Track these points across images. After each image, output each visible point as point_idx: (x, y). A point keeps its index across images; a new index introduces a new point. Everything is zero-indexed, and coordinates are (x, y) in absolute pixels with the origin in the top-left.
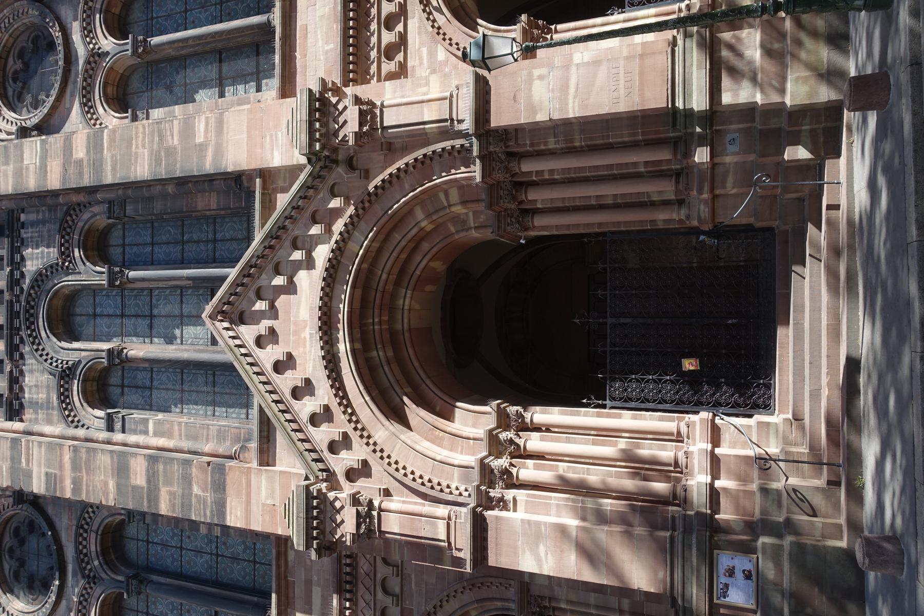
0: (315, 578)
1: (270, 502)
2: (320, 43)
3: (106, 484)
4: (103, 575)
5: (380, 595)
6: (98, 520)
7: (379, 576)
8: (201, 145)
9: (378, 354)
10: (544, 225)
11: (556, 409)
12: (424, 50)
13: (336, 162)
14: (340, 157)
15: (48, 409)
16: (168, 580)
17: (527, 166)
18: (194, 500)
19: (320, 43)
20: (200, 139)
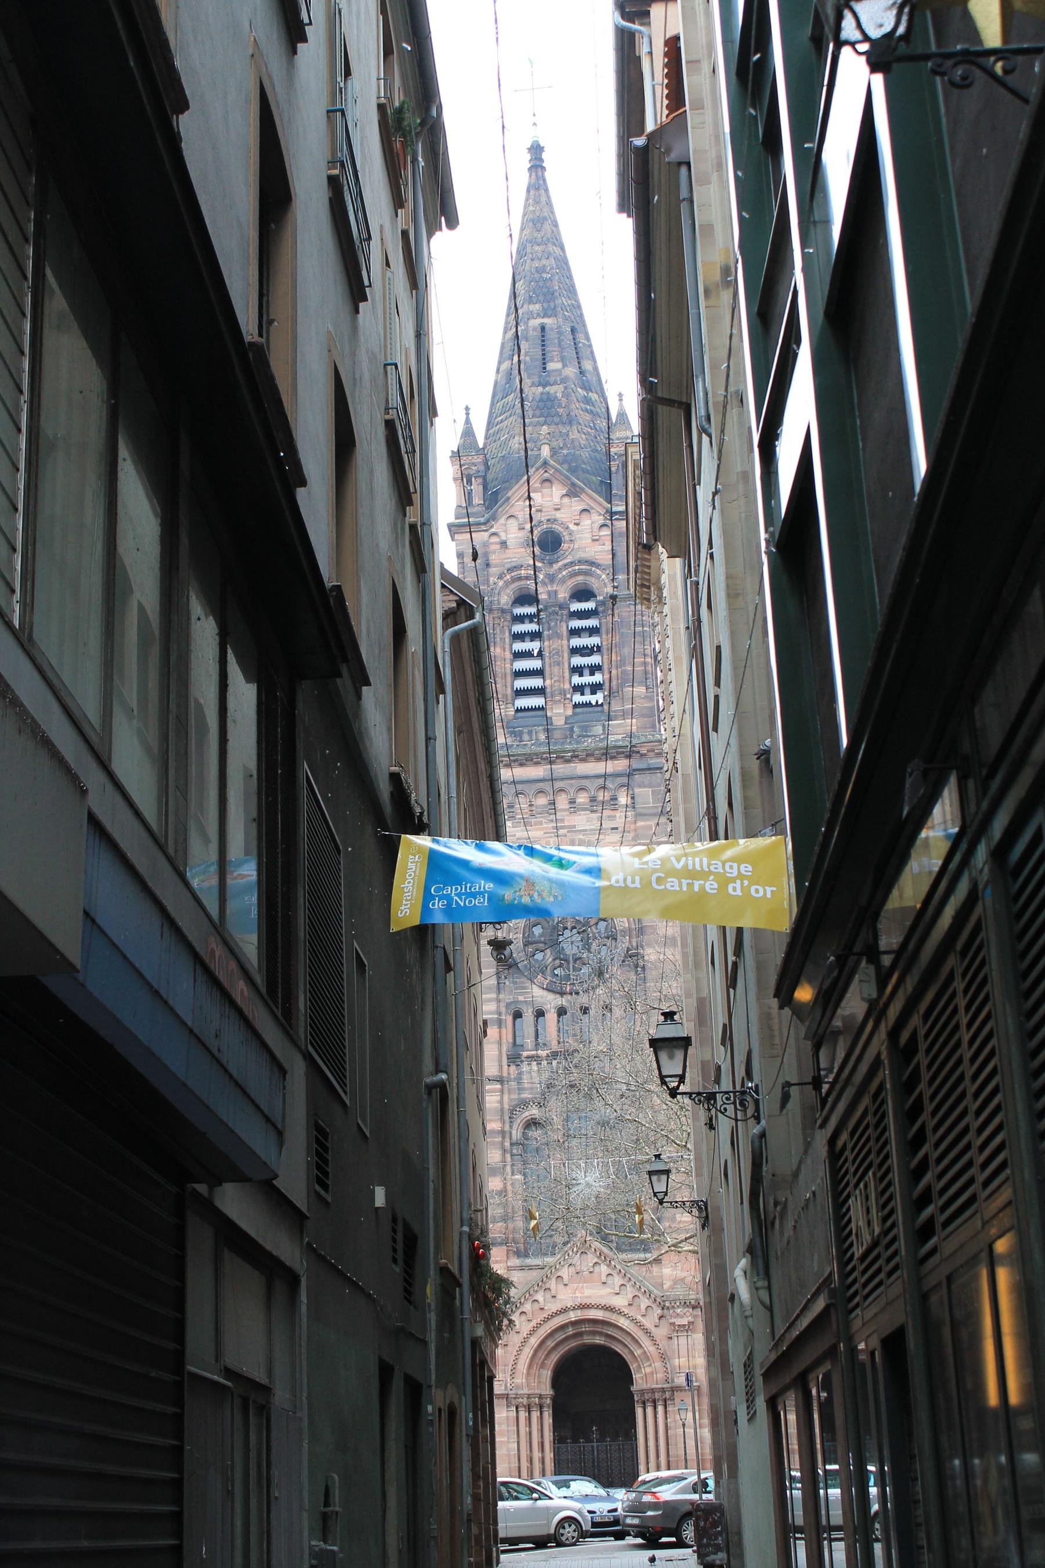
9: (570, 1331)
10: (639, 1411)
13: (663, 1309)
14: (665, 1311)
15: (519, 1089)
17: (660, 1409)
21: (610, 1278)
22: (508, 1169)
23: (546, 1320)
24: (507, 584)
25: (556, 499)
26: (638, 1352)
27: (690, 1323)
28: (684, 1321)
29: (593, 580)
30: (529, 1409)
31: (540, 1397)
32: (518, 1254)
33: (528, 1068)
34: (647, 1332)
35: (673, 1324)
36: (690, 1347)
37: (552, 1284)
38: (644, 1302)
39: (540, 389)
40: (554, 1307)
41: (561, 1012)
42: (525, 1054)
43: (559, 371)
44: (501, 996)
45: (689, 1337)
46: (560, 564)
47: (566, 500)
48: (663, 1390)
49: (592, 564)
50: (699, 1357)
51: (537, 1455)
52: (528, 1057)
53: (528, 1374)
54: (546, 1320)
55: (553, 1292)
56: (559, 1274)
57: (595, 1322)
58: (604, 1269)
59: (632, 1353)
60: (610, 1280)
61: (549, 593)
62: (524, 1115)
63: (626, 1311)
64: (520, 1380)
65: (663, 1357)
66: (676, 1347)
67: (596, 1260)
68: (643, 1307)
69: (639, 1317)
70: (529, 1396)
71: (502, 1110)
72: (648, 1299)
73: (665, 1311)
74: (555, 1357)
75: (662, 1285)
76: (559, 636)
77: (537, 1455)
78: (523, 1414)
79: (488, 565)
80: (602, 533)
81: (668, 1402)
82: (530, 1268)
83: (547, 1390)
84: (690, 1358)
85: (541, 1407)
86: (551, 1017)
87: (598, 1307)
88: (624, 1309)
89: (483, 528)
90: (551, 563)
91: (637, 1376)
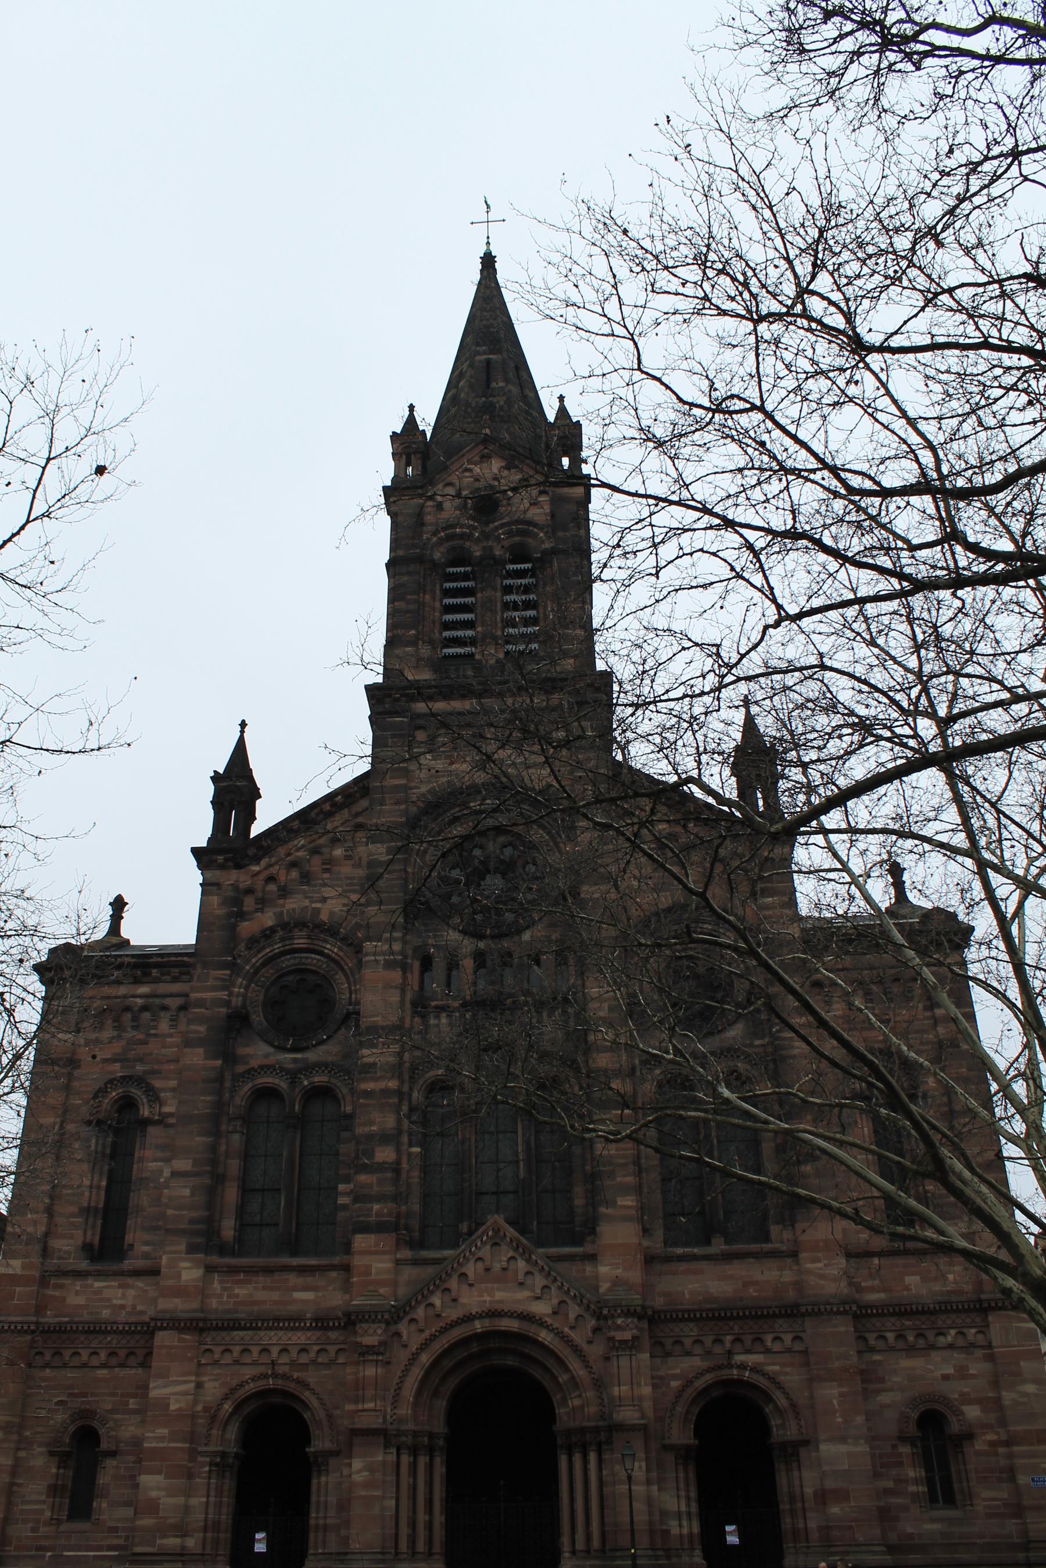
0: (320, 1294)
1: (373, 1270)
2: (690, 1286)
3: (372, 1123)
4: (297, 1090)
5: (316, 1348)
6: (339, 1084)
7: (328, 1347)
8: (615, 1202)
9: (475, 1348)
10: (563, 1460)
11: (444, 1470)
12: (678, 1371)
13: (598, 1319)
16: (298, 1149)
17: (592, 1456)
18: (369, 1205)
19: (690, 1286)
20: (621, 1201)
21: (529, 1277)
22: (405, 1139)
23: (443, 1330)
24: (441, 541)
25: (495, 470)
26: (563, 1378)
27: (635, 1338)
28: (627, 1335)
29: (530, 540)
30: (414, 1452)
31: (431, 1435)
32: (412, 1244)
33: (436, 1022)
34: (576, 1350)
35: (611, 1339)
36: (634, 1371)
37: (453, 1283)
38: (573, 1310)
39: (484, 399)
40: (453, 1314)
41: (480, 958)
42: (433, 1004)
43: (503, 388)
44: (408, 938)
45: (634, 1358)
46: (496, 524)
47: (505, 473)
48: (597, 1430)
49: (530, 523)
50: (646, 1385)
51: (422, 1517)
52: (436, 1007)
53: (416, 1404)
54: (443, 1330)
55: (454, 1294)
56: (463, 1270)
57: (506, 1335)
58: (522, 1265)
59: (555, 1378)
60: (529, 1281)
61: (484, 548)
62: (428, 1075)
63: (549, 1321)
64: (405, 1410)
65: (599, 1384)
66: (615, 1370)
67: (511, 1254)
68: (572, 1316)
69: (566, 1329)
70: (415, 1434)
71: (401, 1063)
72: (579, 1305)
73: (602, 1322)
74: (452, 1383)
75: (597, 1288)
76: (494, 589)
77: (422, 1517)
78: (406, 1459)
79: (423, 524)
80: (540, 499)
81: (604, 1447)
82: (426, 1262)
83: (440, 1427)
84: (635, 1387)
85: (431, 1451)
86: (468, 963)
87: (511, 1315)
88: (547, 1319)
89: (420, 491)
90: (487, 523)
91: (561, 1411)
